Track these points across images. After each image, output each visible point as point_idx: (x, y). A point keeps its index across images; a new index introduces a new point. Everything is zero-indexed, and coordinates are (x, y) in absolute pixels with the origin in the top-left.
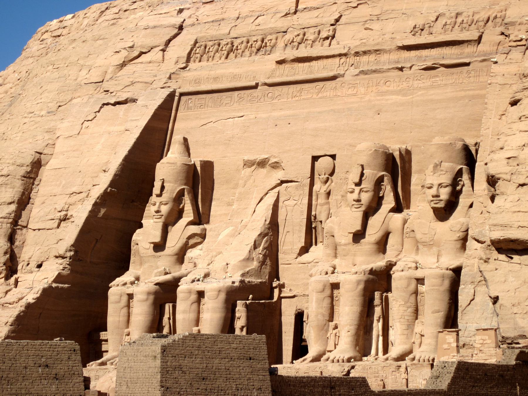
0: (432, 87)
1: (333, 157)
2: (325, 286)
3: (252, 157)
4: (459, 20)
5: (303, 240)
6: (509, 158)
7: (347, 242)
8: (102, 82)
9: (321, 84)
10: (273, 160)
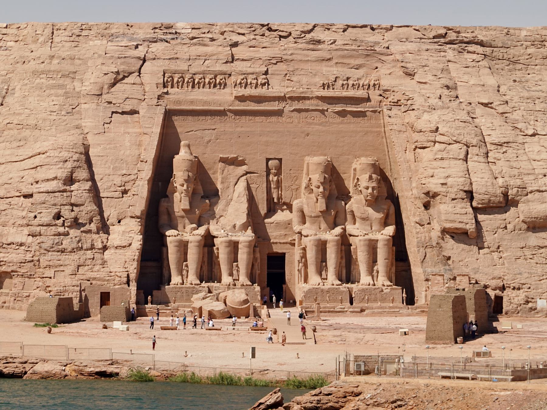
0: (342, 123)
1: (280, 160)
4: (351, 82)
6: (442, 184)
7: (315, 215)
8: (101, 95)
10: (240, 159)
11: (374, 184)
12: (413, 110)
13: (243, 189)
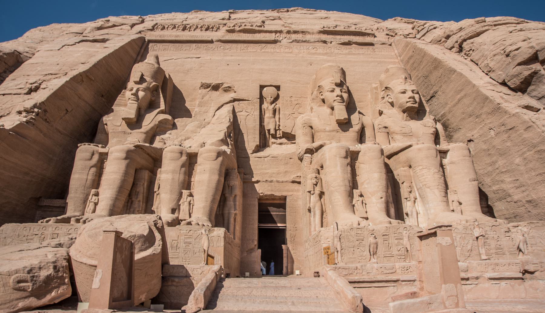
0: (349, 54)
1: (278, 88)
2: (347, 152)
3: (208, 82)
5: (257, 140)
7: (331, 129)
9: (264, 45)
10: (226, 85)
11: (414, 87)
12: (435, 28)
13: (227, 111)
